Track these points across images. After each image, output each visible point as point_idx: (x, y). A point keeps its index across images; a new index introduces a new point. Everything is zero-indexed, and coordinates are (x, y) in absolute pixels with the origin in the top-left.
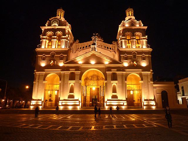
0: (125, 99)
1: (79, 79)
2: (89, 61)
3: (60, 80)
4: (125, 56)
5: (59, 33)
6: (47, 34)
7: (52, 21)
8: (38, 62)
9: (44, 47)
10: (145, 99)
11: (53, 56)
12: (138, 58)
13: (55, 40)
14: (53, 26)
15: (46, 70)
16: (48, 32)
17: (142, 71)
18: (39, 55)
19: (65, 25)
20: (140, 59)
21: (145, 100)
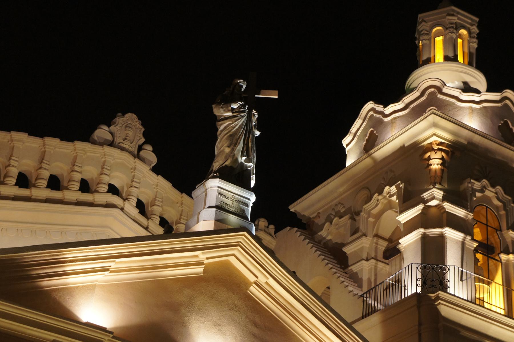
2: (183, 325)
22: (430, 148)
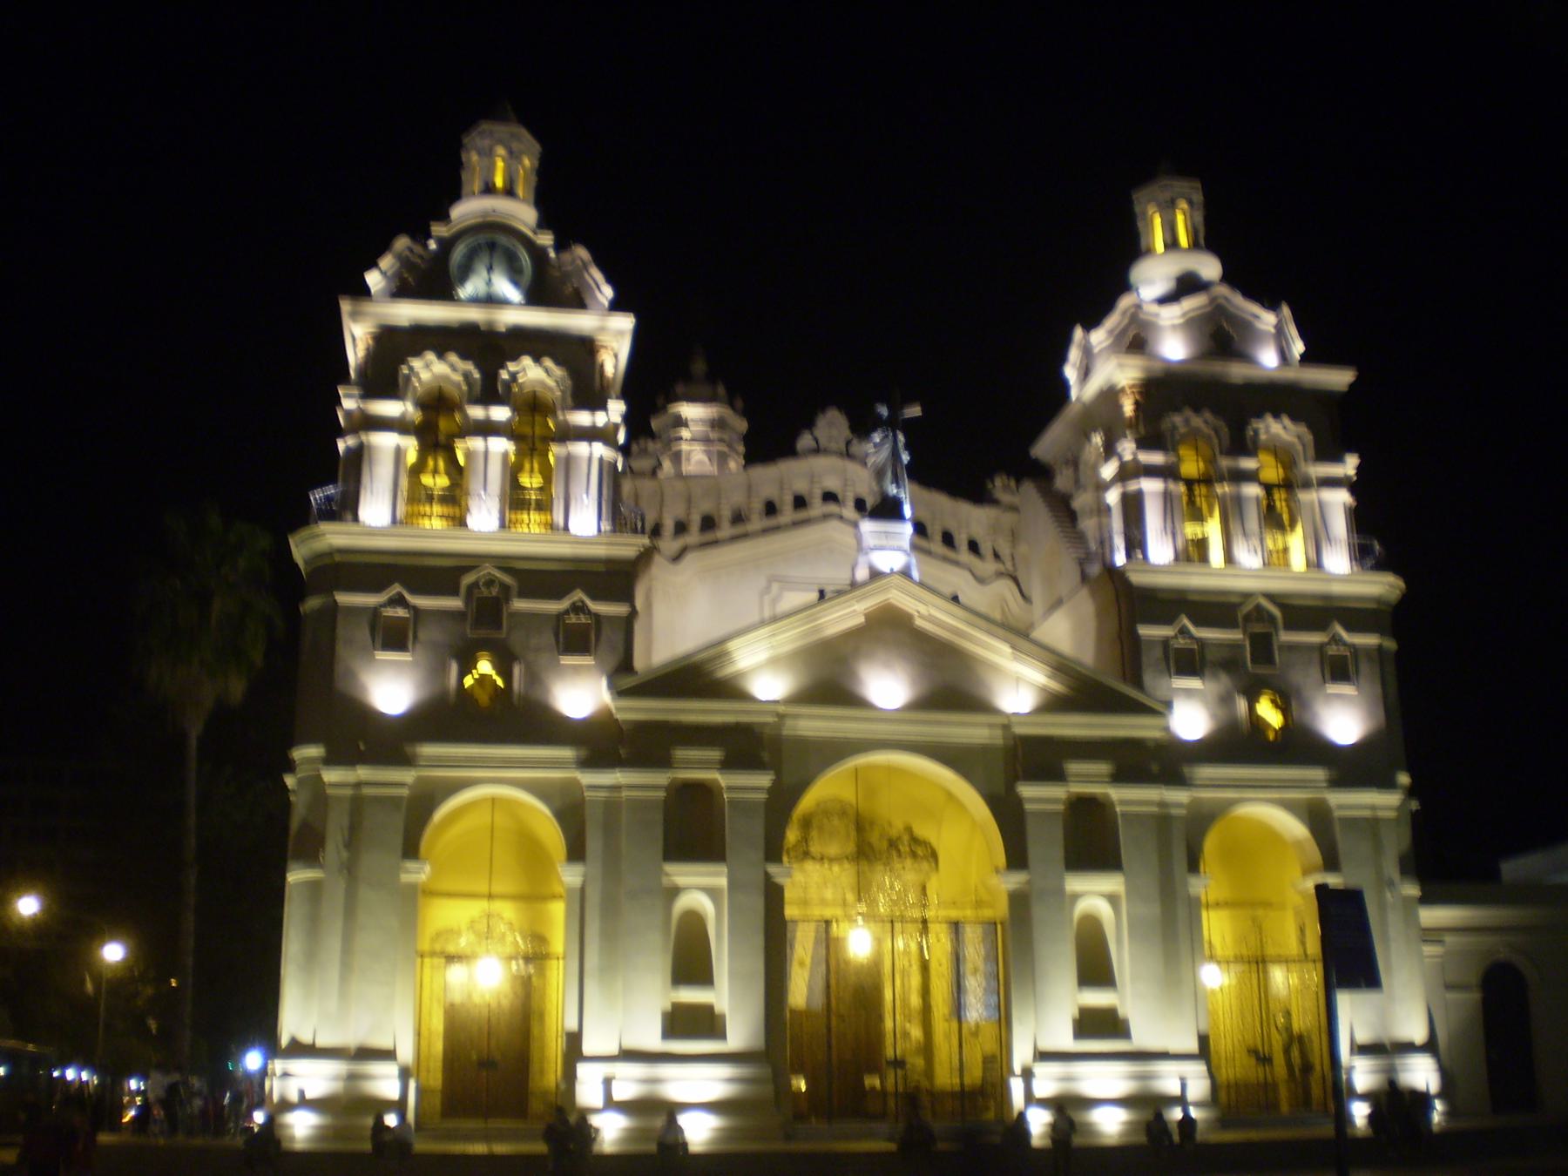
0: (1192, 1045)
1: (761, 855)
2: (852, 675)
3: (576, 853)
4: (1181, 643)
5: (531, 373)
6: (408, 379)
8: (339, 669)
10: (1363, 1037)
14: (475, 301)
16: (416, 363)
17: (1338, 783)
18: (344, 599)
19: (577, 301)
20: (1305, 676)
21: (1362, 1050)
22: (1123, 390)
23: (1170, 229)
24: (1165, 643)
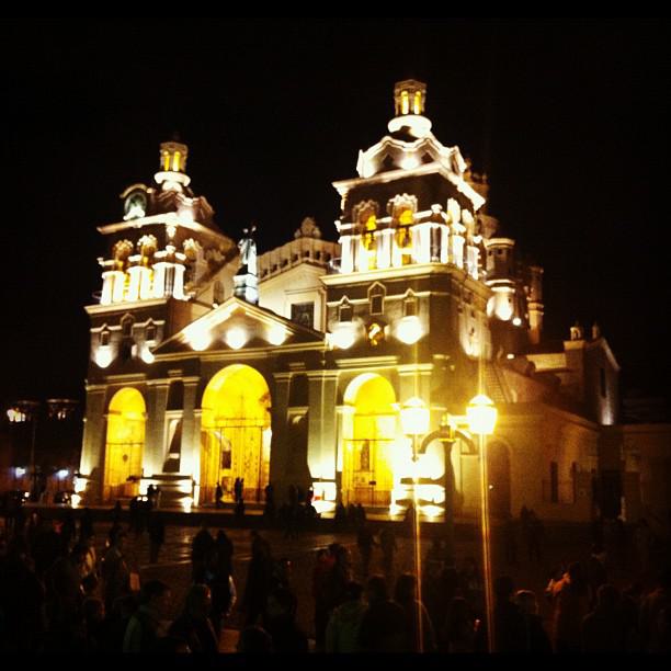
0: (333, 477)
2: (224, 336)
4: (344, 307)
7: (128, 201)
9: (110, 303)
11: (127, 329)
12: (389, 310)
13: (116, 273)
15: (110, 378)
23: (411, 103)
24: (337, 307)
